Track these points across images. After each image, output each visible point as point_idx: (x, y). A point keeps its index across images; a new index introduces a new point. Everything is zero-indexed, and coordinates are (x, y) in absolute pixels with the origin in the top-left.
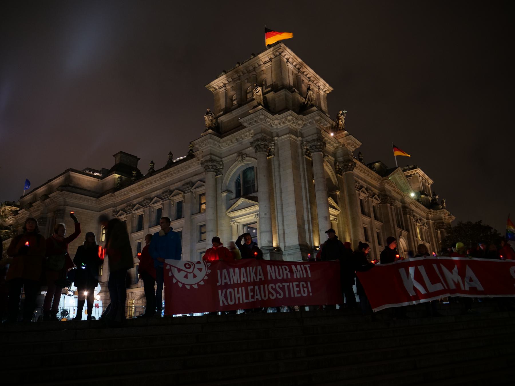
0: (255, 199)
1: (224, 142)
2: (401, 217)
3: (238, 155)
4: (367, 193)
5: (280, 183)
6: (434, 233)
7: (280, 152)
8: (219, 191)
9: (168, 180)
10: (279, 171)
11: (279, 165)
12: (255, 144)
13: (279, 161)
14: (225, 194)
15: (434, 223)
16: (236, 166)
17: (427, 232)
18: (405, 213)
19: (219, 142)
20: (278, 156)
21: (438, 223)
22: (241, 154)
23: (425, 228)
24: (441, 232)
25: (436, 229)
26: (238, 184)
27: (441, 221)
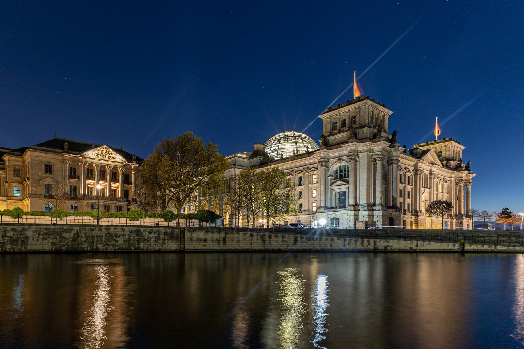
0: (347, 182)
1: (331, 152)
2: (427, 180)
3: (338, 160)
4: (405, 170)
5: (360, 175)
6: (454, 186)
7: (361, 160)
8: (327, 176)
9: (294, 165)
10: (360, 170)
11: (360, 167)
12: (349, 157)
13: (360, 165)
14: (330, 178)
15: (456, 180)
16: (336, 164)
17: (448, 186)
18: (431, 178)
19: (328, 152)
20: (360, 163)
21: (458, 180)
22: (340, 159)
23: (446, 184)
24: (460, 186)
25: (456, 184)
26: (336, 172)
27: (461, 179)
